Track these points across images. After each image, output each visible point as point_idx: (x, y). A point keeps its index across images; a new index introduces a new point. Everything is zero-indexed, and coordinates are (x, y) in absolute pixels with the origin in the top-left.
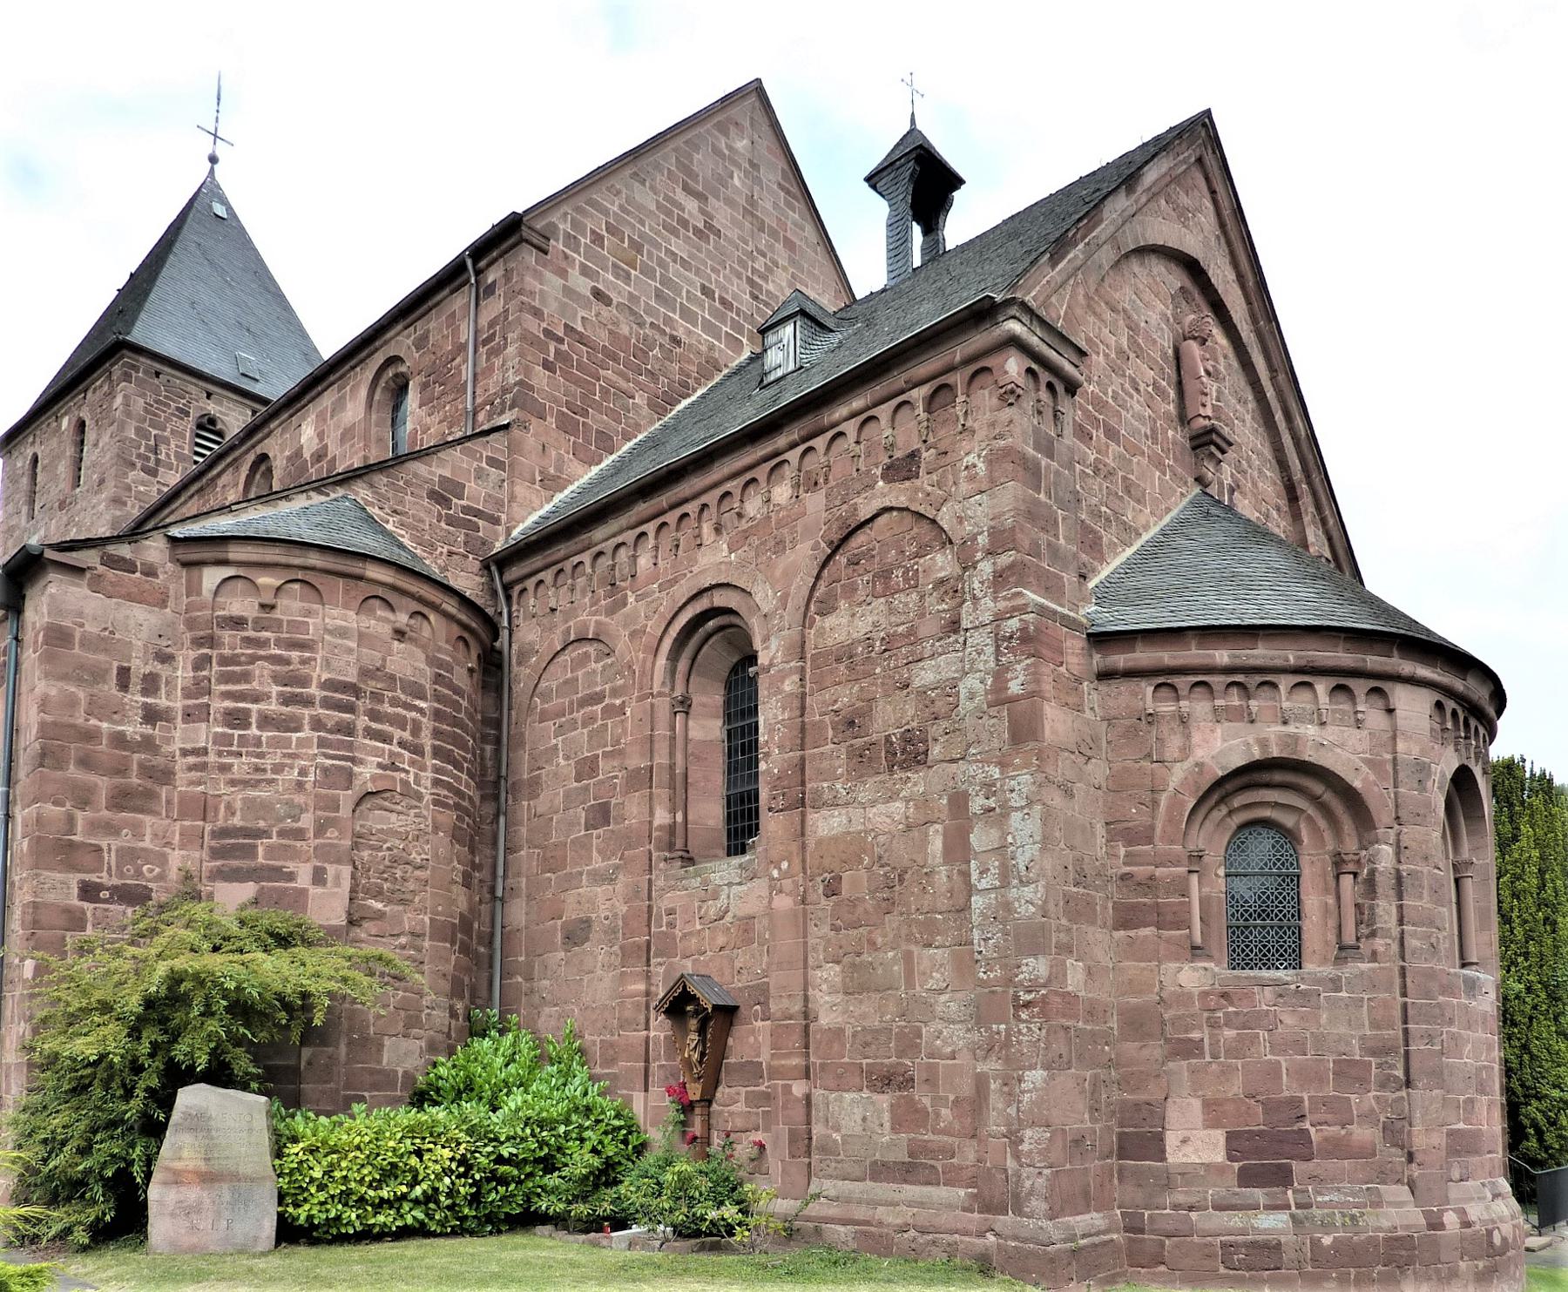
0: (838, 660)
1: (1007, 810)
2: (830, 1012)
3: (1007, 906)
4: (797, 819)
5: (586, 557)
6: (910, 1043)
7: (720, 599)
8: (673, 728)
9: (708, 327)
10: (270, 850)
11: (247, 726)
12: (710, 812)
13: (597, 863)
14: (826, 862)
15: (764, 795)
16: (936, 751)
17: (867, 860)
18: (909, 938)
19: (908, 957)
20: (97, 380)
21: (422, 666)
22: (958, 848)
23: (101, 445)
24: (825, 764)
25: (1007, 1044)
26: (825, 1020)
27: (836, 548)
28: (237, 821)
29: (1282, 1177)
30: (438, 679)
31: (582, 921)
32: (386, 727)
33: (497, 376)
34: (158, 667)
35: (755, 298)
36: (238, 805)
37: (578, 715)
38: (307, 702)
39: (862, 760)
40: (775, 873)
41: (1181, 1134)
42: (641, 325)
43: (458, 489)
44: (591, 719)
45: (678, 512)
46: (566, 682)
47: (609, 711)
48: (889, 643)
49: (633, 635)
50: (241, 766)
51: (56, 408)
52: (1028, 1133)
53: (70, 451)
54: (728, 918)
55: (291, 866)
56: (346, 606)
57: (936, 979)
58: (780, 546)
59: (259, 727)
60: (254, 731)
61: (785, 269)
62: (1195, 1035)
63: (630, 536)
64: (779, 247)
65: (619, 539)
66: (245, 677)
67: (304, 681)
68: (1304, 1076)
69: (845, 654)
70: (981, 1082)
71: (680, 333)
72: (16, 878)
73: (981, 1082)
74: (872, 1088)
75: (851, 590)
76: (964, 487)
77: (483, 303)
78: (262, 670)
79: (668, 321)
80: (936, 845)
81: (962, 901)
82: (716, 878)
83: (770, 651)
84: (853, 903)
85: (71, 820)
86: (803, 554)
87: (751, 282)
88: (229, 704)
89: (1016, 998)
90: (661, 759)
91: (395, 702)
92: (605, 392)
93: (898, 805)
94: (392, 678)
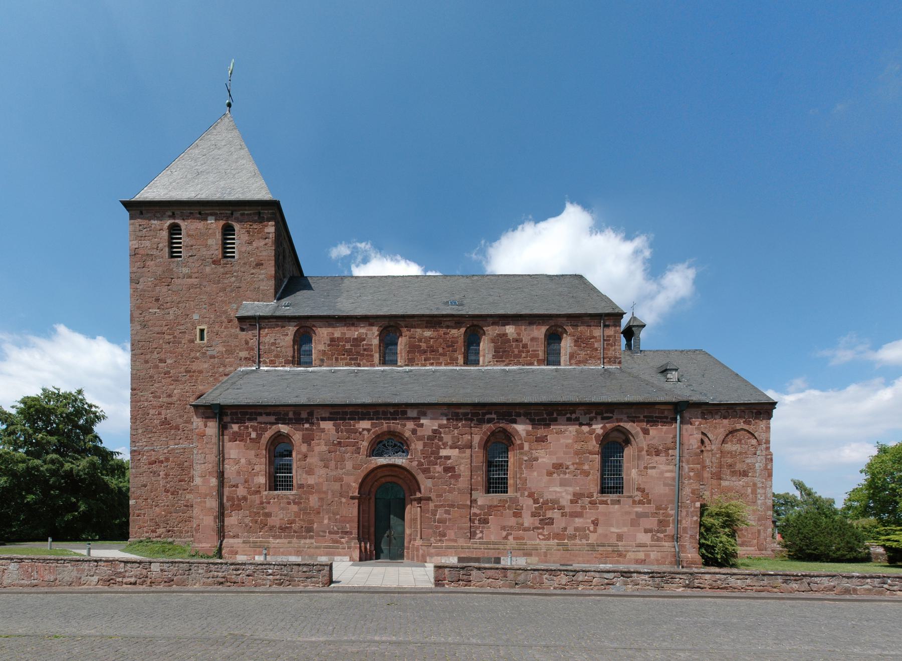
0: (728, 453)
16: (750, 474)
20: (246, 210)
22: (754, 492)
23: (255, 244)
48: (741, 453)
51: (202, 208)
53: (219, 236)
69: (730, 452)
70: (759, 531)
76: (760, 430)
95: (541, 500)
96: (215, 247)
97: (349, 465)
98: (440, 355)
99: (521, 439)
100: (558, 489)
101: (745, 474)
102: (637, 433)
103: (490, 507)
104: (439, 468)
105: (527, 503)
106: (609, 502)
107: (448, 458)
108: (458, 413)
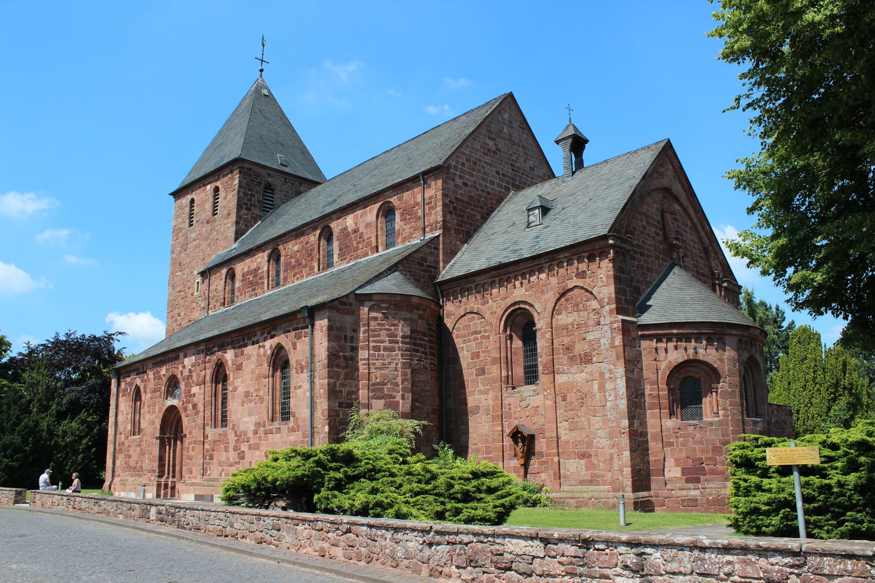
0: (563, 329)
1: (616, 378)
2: (564, 436)
3: (617, 405)
4: (552, 377)
5: (473, 285)
6: (590, 444)
7: (522, 306)
8: (507, 345)
9: (499, 186)
10: (388, 389)
11: (380, 351)
12: (519, 371)
13: (481, 387)
14: (562, 390)
15: (540, 368)
16: (594, 359)
17: (575, 391)
18: (589, 414)
19: (589, 420)
21: (425, 325)
22: (602, 388)
24: (560, 361)
25: (618, 444)
26: (563, 438)
27: (563, 295)
28: (378, 380)
29: (698, 480)
30: (430, 330)
31: (476, 406)
32: (418, 348)
33: (433, 217)
34: (353, 334)
35: (513, 170)
36: (378, 375)
37: (472, 337)
38: (397, 342)
39: (572, 359)
40: (546, 393)
41: (668, 469)
42: (478, 190)
43: (425, 260)
44: (477, 339)
45: (507, 276)
46: (466, 326)
47: (483, 337)
49: (491, 313)
50: (379, 363)
52: (625, 469)
54: (530, 407)
55: (394, 394)
56: (406, 311)
57: (597, 426)
58: (543, 292)
59: (384, 351)
60: (382, 352)
61: (522, 156)
62: (672, 440)
63: (489, 280)
64: (520, 149)
65: (485, 281)
66: (379, 335)
67: (396, 336)
68: (703, 451)
69: (565, 328)
70: (611, 456)
71: (490, 190)
72: (318, 401)
73: (611, 456)
74: (579, 458)
75: (566, 308)
77: (426, 190)
78: (383, 333)
79: (486, 187)
80: (596, 387)
81: (604, 404)
82: (525, 394)
83: (541, 324)
84: (571, 403)
85: (335, 383)
86: (551, 296)
87: (512, 165)
88: (374, 344)
89: (620, 431)
90: (503, 355)
91: (420, 339)
92: (467, 217)
93: (583, 374)
94: (419, 331)
95: (238, 432)
96: (208, 209)
97: (157, 407)
98: (303, 267)
99: (229, 370)
100: (246, 419)
101: (586, 359)
102: (290, 348)
103: (215, 442)
104: (190, 406)
105: (231, 436)
106: (274, 432)
107: (194, 395)
108: (199, 350)
